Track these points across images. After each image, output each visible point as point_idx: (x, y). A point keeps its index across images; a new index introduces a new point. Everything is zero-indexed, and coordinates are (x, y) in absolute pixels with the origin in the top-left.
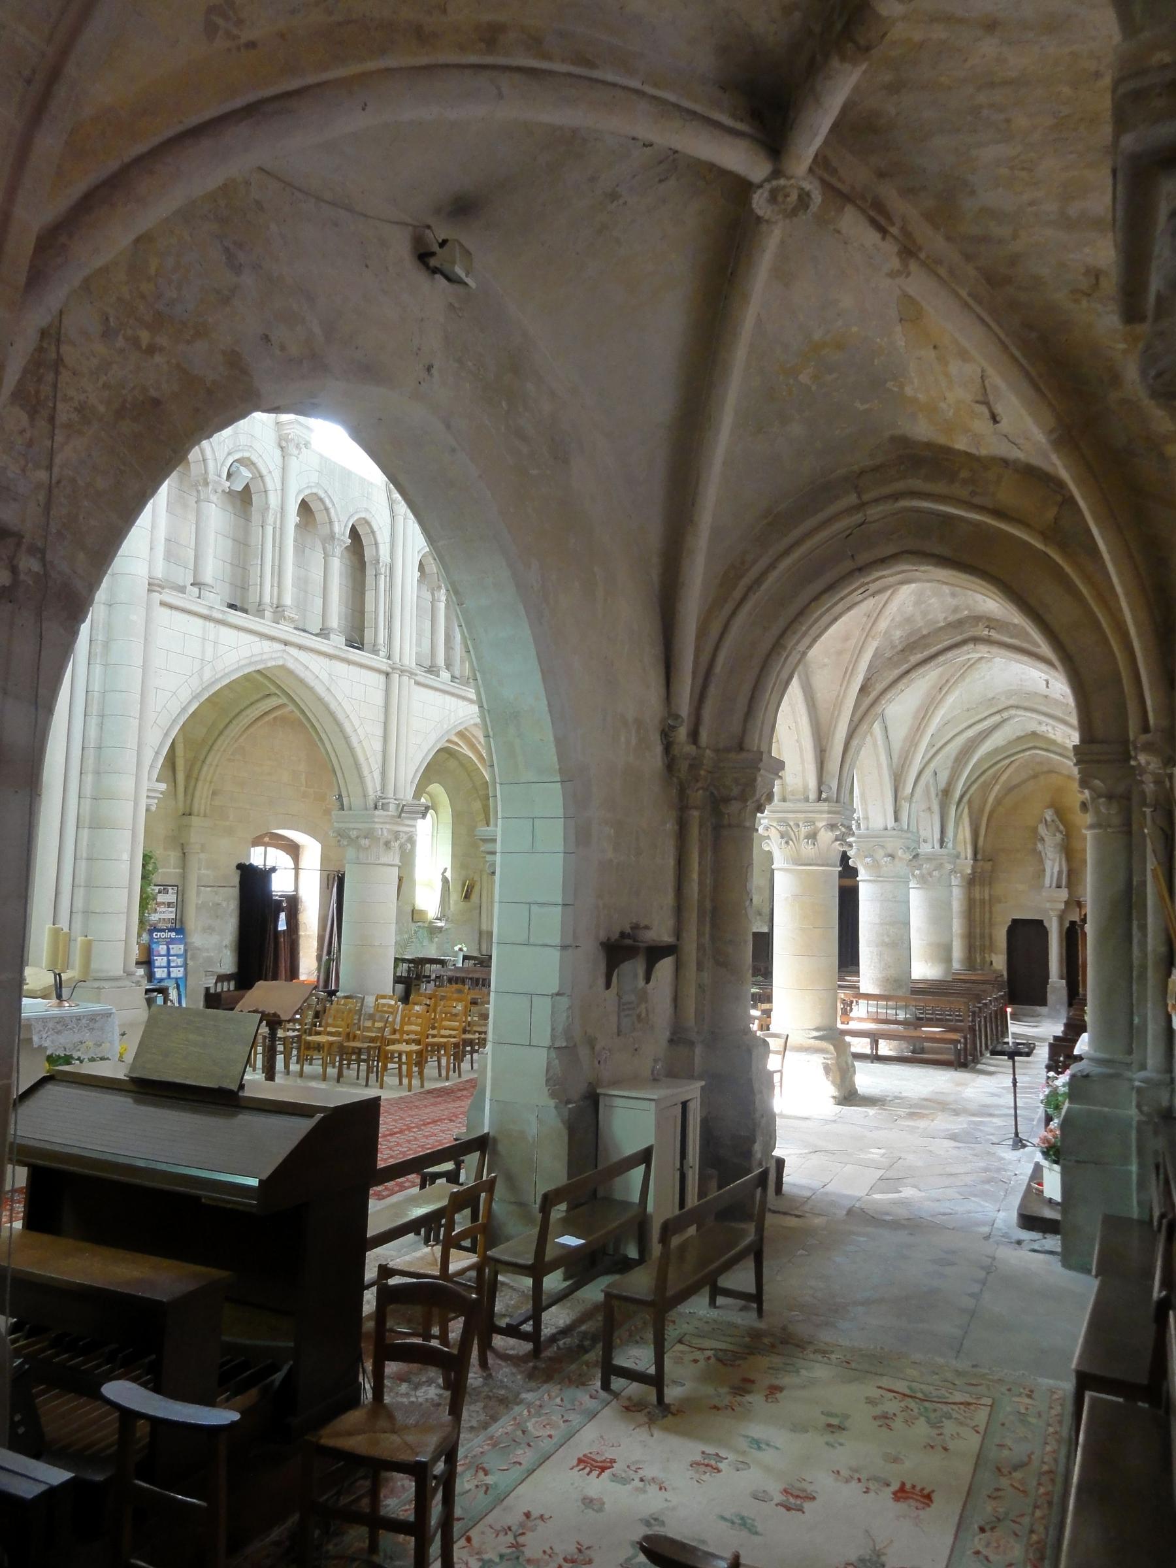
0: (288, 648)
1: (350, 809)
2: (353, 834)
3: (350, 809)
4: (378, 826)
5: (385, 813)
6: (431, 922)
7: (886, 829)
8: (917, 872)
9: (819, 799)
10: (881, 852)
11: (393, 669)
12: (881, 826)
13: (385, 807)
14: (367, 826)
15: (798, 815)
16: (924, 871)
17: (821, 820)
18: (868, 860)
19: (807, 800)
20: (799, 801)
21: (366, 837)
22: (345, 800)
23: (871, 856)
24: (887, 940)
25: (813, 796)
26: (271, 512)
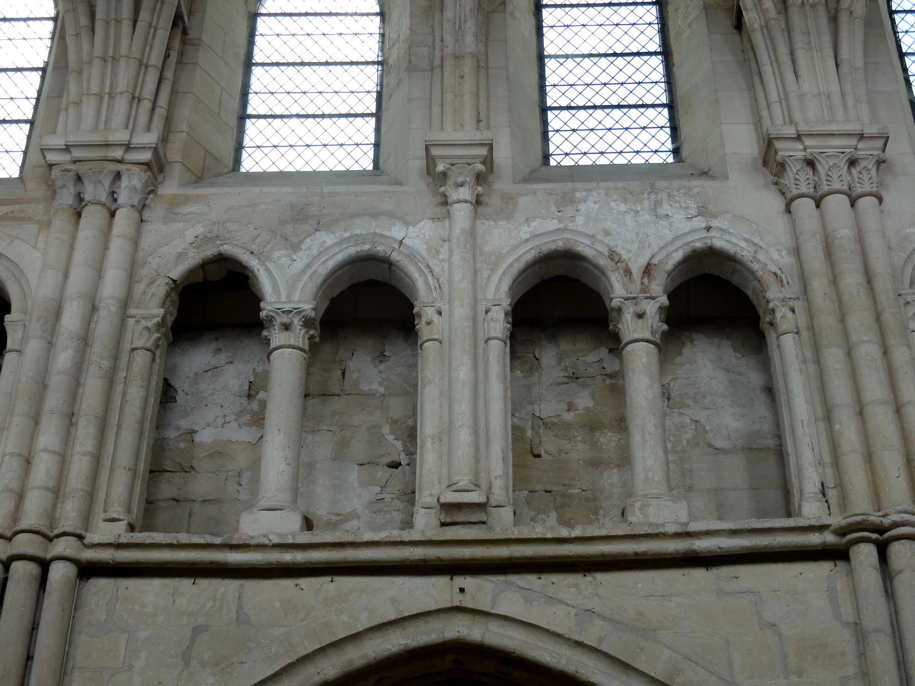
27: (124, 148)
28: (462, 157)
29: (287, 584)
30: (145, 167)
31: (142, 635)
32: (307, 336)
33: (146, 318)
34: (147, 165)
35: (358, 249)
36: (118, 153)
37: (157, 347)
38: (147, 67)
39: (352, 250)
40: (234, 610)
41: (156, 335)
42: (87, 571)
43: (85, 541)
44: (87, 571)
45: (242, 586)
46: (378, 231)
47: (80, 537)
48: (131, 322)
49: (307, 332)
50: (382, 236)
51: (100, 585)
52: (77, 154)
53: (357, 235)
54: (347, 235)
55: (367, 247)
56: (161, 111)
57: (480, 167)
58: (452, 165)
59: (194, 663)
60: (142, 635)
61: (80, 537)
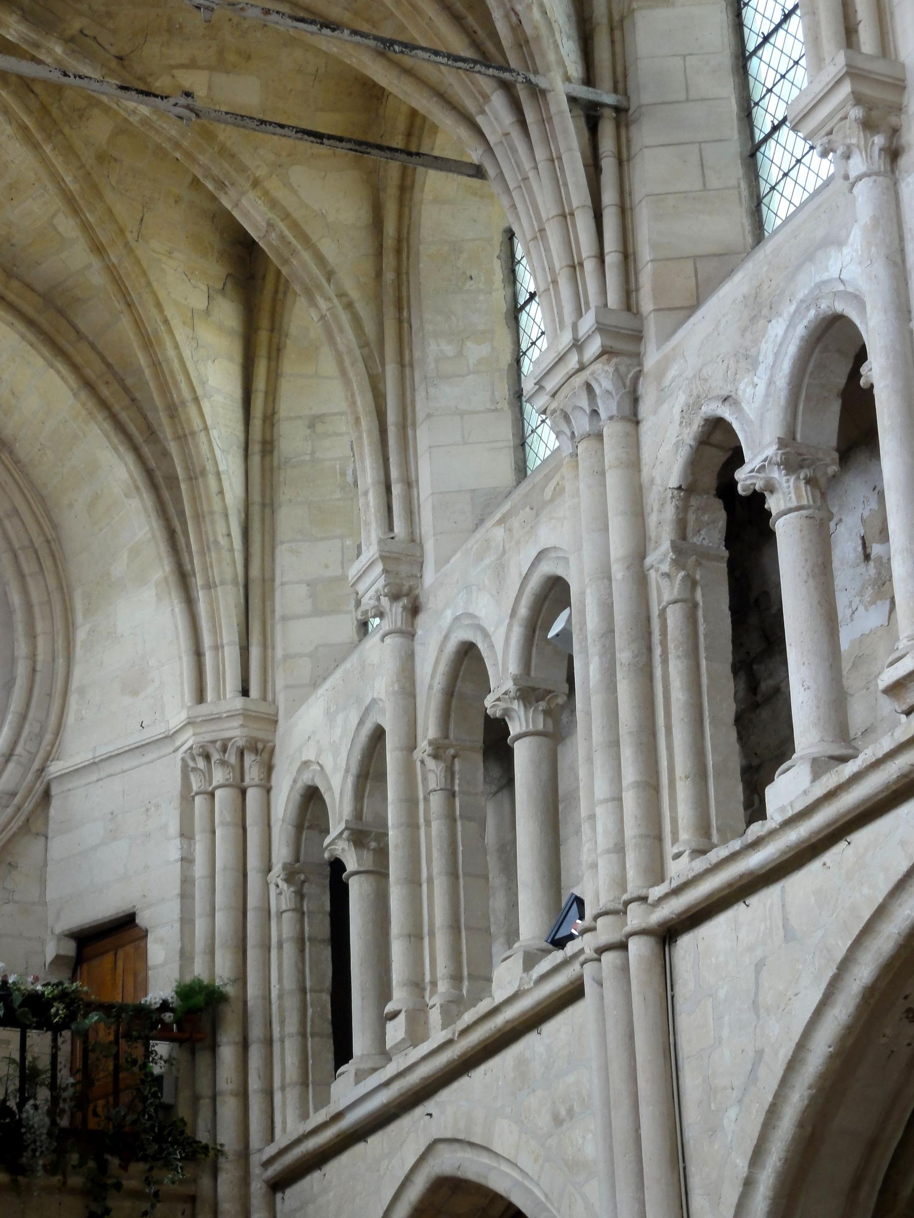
27: (574, 350)
28: (831, 116)
29: (814, 867)
30: (605, 357)
31: (722, 994)
32: (802, 483)
33: (661, 561)
34: (606, 352)
35: (805, 322)
36: (573, 362)
37: (694, 584)
38: (572, 214)
39: (800, 330)
40: (780, 925)
41: (682, 574)
42: (667, 935)
43: (650, 901)
44: (667, 935)
45: (783, 890)
46: (818, 279)
47: (643, 899)
48: (653, 574)
49: (798, 478)
50: (824, 283)
51: (685, 942)
52: (551, 384)
53: (802, 301)
54: (792, 308)
55: (812, 313)
56: (612, 258)
57: (856, 113)
58: (830, 133)
59: (762, 1011)
60: (722, 994)
61: (643, 899)
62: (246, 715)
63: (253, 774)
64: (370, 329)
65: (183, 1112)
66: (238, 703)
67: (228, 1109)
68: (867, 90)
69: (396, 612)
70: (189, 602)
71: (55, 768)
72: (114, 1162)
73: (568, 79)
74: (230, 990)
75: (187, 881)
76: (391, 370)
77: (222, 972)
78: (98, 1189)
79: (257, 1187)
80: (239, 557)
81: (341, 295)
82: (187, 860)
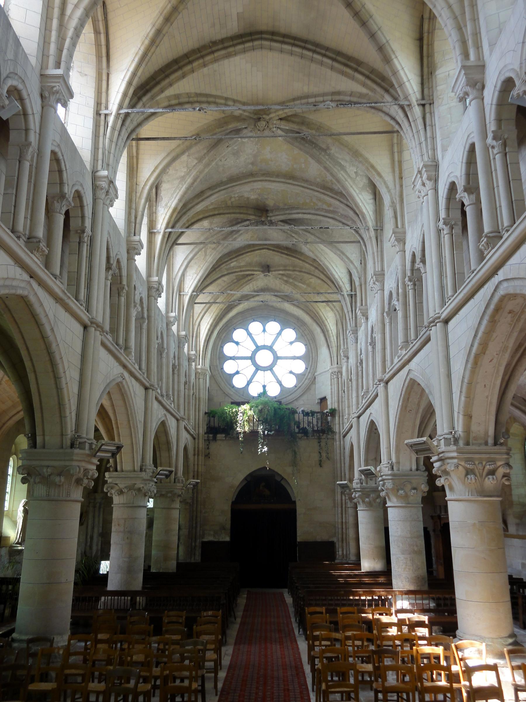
0: (32, 281)
1: (44, 447)
2: (46, 472)
3: (44, 447)
4: (75, 463)
5: (81, 451)
6: (11, 547)
7: (411, 470)
8: (367, 500)
9: (495, 444)
10: (409, 486)
11: (92, 323)
12: (409, 468)
13: (81, 446)
14: (62, 463)
15: (483, 456)
16: (371, 499)
17: (500, 460)
18: (401, 492)
19: (486, 444)
20: (480, 444)
21: (60, 475)
22: (39, 439)
23: (402, 489)
24: (416, 549)
25: (491, 441)
26: (31, 149)
44: (359, 417)
62: (337, 367)
63: (339, 376)
64: (341, 315)
65: (332, 426)
66: (336, 365)
67: (337, 426)
68: (362, 311)
69: (345, 359)
70: (330, 350)
71: (316, 374)
72: (321, 434)
73: (347, 291)
74: (337, 409)
75: (332, 392)
76: (344, 321)
77: (336, 407)
78: (319, 438)
79: (342, 437)
80: (336, 342)
81: (337, 310)
82: (331, 389)
